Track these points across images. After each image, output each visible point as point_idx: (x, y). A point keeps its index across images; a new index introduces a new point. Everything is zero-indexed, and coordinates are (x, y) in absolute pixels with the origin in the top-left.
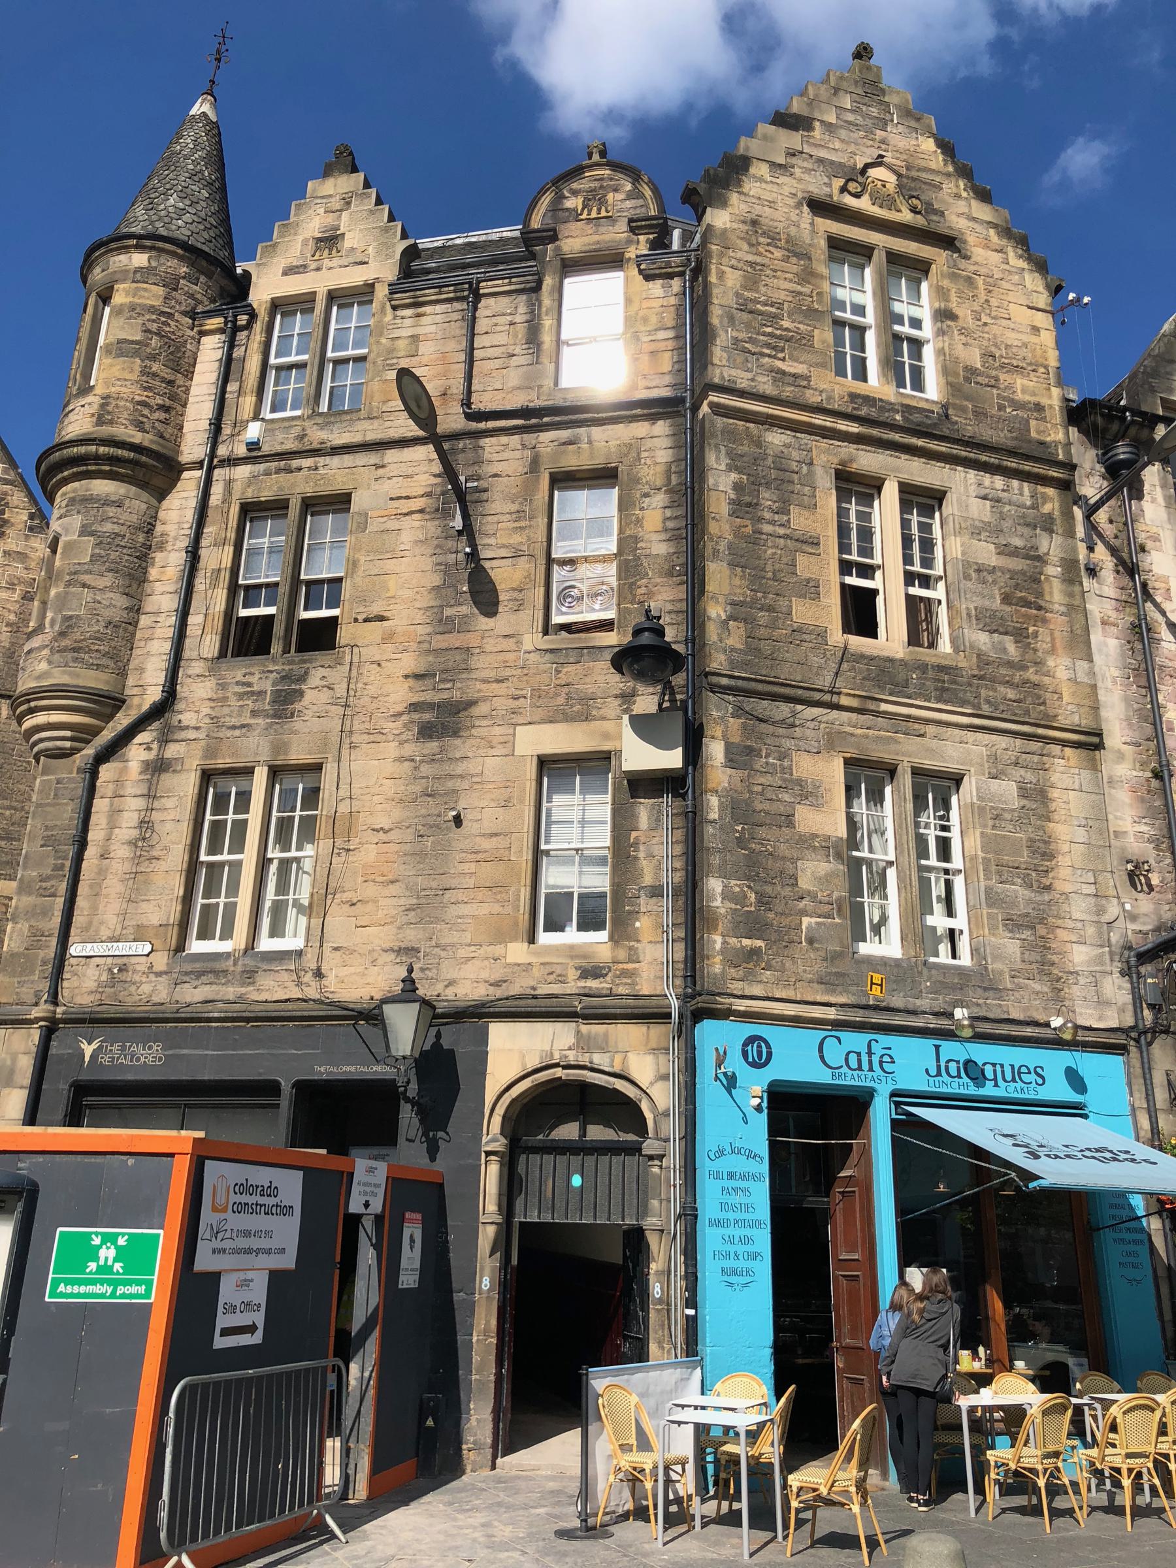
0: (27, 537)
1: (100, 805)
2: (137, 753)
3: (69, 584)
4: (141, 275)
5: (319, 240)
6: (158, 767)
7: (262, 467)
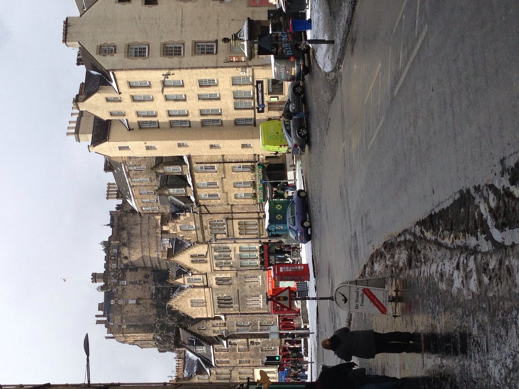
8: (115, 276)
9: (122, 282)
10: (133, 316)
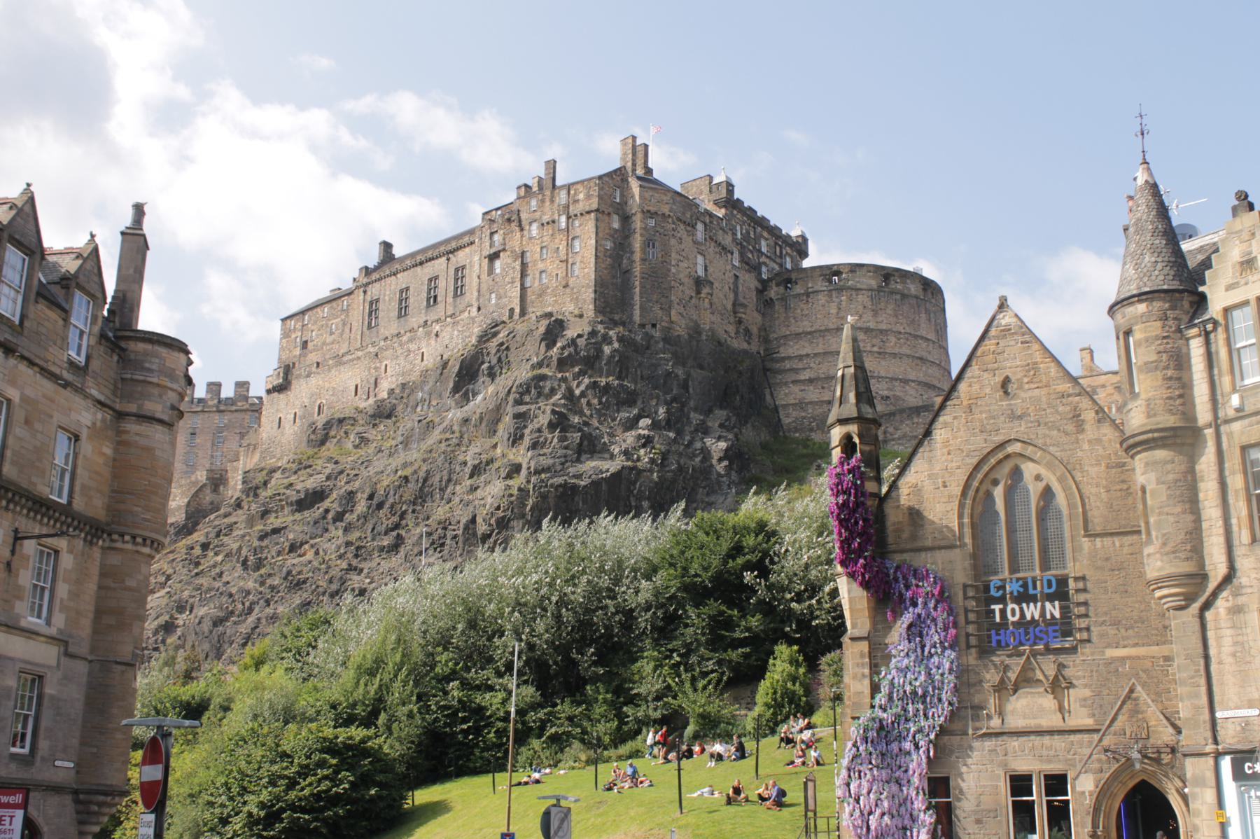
0: (1098, 428)
1: (1210, 634)
2: (1222, 604)
3: (1160, 514)
4: (1144, 318)
5: (1242, 263)
6: (1237, 610)
7: (1247, 421)
8: (746, 237)
9: (736, 255)
10: (667, 254)
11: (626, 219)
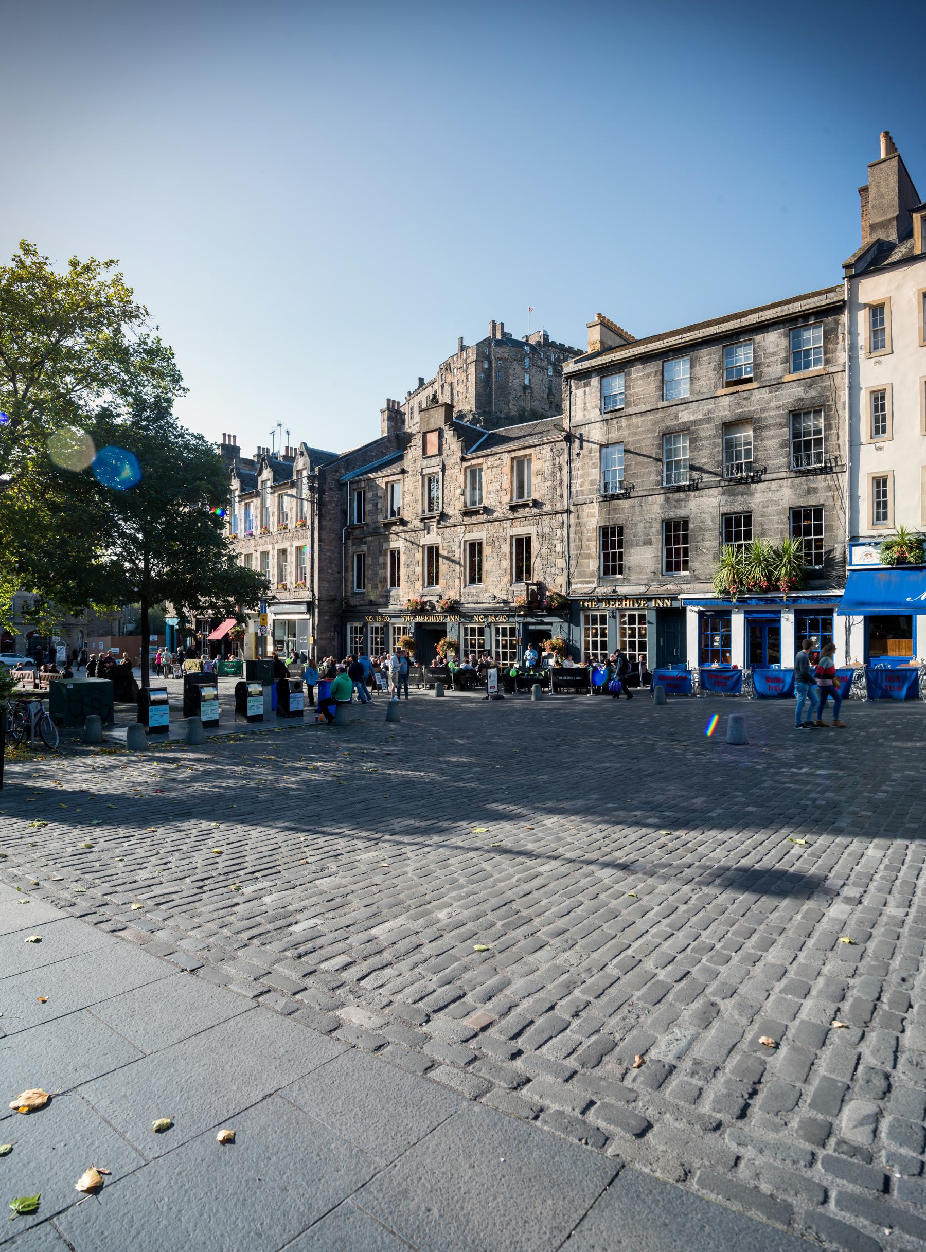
9: (551, 369)
10: (507, 377)
11: (490, 363)
